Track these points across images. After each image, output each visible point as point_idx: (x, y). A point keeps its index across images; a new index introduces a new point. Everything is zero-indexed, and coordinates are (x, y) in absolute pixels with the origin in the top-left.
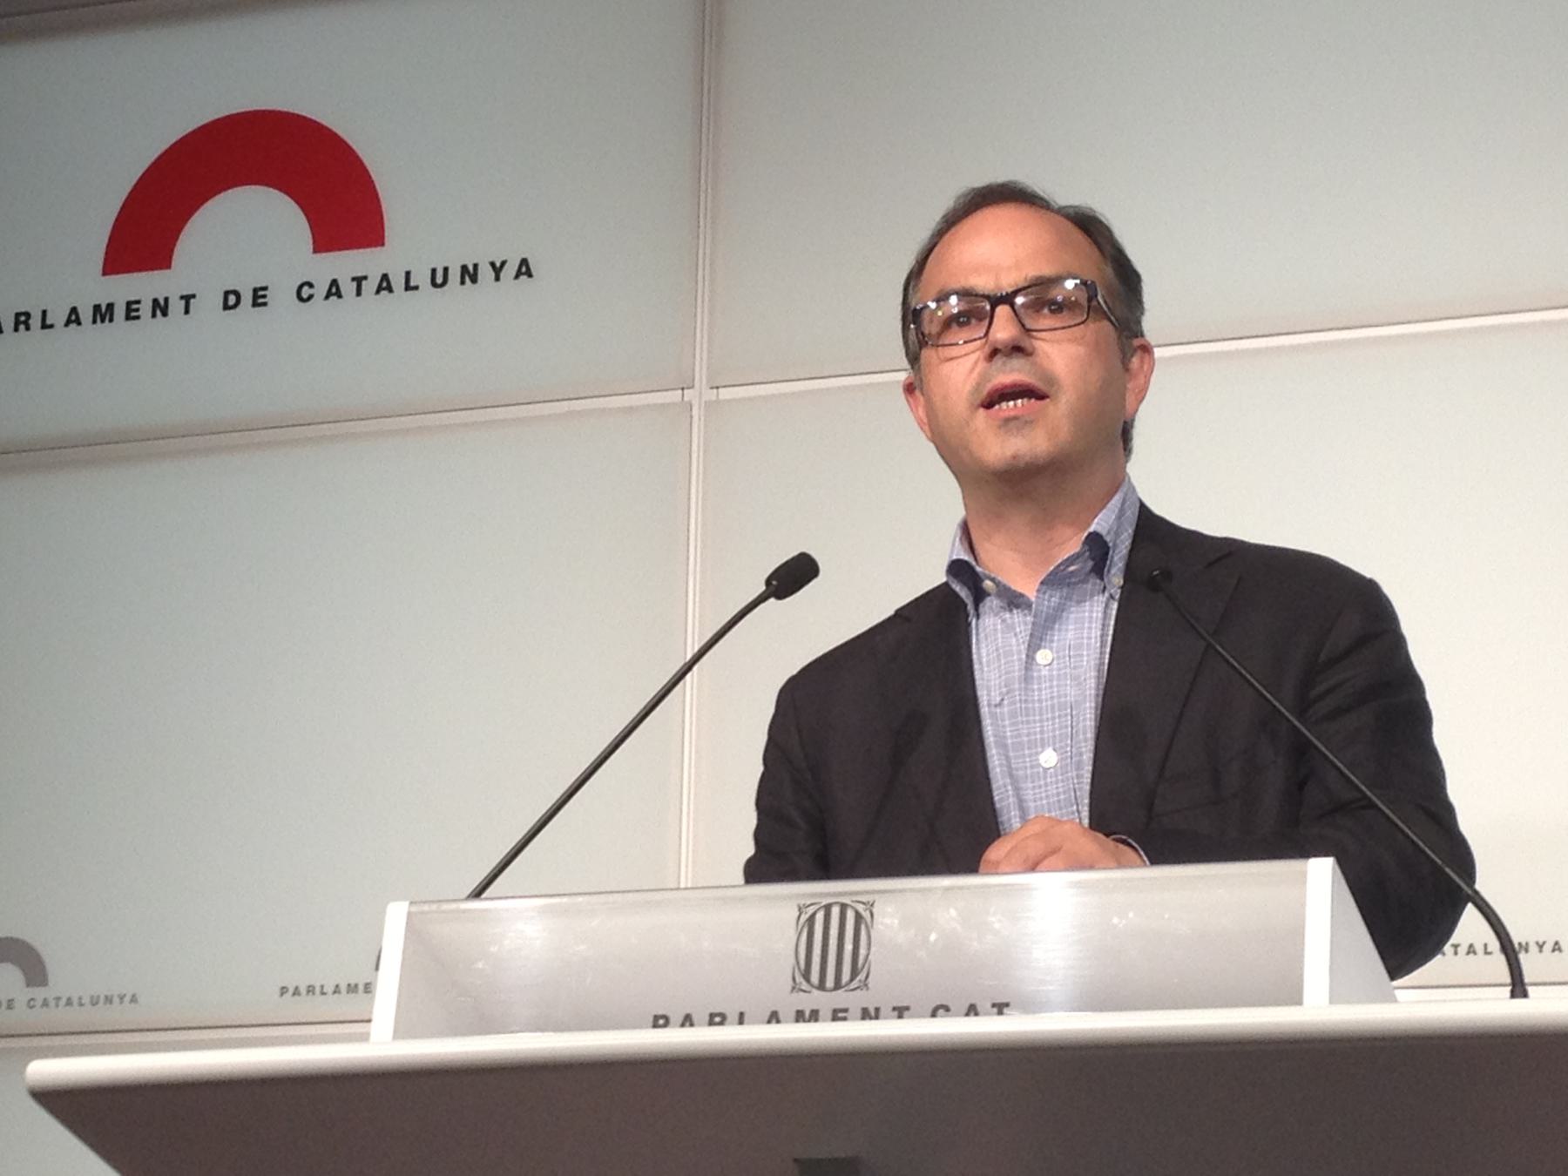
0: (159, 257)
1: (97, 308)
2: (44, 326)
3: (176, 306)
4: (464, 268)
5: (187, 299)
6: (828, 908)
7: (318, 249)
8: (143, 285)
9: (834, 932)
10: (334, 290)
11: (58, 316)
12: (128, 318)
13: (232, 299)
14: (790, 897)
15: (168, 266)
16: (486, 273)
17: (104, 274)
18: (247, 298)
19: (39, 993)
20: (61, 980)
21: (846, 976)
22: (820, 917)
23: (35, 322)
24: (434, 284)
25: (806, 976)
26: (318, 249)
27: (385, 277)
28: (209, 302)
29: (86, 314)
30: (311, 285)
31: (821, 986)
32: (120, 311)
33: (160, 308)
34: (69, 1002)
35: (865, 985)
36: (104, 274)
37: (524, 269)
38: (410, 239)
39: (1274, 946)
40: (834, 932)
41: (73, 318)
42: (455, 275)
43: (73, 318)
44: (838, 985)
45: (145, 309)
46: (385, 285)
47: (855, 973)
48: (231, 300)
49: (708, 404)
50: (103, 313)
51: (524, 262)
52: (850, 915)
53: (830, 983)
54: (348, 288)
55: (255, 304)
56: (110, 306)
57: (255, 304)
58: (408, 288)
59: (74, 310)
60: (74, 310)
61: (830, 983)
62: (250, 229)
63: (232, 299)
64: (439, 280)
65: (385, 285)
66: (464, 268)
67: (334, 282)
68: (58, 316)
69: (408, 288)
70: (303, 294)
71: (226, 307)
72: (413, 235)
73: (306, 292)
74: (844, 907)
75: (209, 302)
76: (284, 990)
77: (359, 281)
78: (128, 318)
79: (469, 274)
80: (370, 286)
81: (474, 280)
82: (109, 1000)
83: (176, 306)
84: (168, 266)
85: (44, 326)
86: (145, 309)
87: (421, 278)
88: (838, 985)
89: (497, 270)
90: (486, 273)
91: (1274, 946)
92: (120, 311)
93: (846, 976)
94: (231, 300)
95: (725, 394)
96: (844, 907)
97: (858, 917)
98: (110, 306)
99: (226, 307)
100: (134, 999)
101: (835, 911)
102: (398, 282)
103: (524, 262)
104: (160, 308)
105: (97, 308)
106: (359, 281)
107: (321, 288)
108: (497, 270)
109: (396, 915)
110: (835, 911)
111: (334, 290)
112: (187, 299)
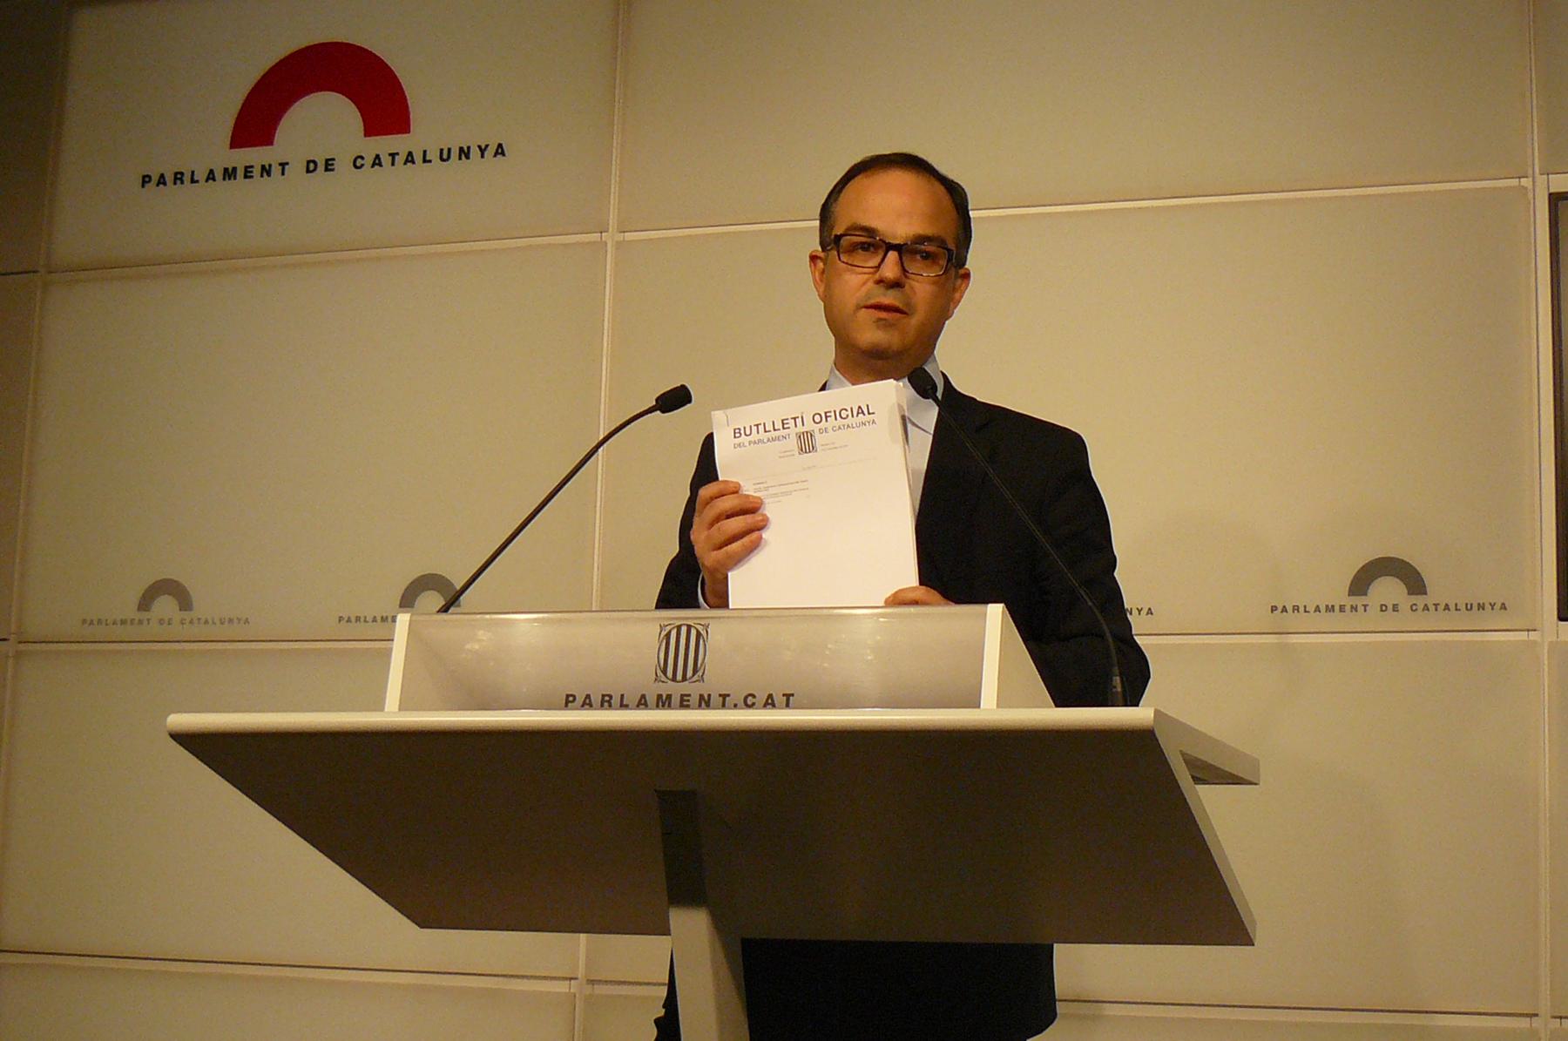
0: (267, 139)
1: (226, 170)
2: (193, 181)
3: (276, 170)
4: (461, 149)
5: (283, 165)
6: (679, 628)
7: (369, 132)
8: (254, 156)
10: (377, 162)
11: (201, 175)
13: (312, 166)
14: (654, 619)
15: (271, 143)
16: (475, 152)
19: (186, 615)
20: (201, 608)
21: (690, 673)
22: (674, 633)
23: (187, 178)
25: (664, 672)
26: (369, 132)
27: (410, 154)
29: (219, 174)
31: (674, 679)
32: (240, 173)
33: (266, 171)
34: (206, 622)
35: (702, 679)
37: (500, 151)
38: (425, 132)
41: (211, 176)
42: (455, 153)
43: (211, 176)
44: (684, 679)
45: (257, 171)
46: (410, 159)
47: (695, 671)
48: (311, 167)
50: (230, 174)
51: (500, 146)
52: (693, 632)
53: (679, 677)
54: (386, 160)
55: (327, 170)
56: (234, 169)
57: (327, 170)
58: (425, 161)
59: (211, 171)
60: (211, 171)
61: (679, 677)
62: (322, 120)
63: (312, 166)
64: (444, 157)
66: (461, 149)
67: (378, 157)
68: (201, 175)
69: (425, 161)
71: (308, 171)
73: (359, 162)
74: (689, 627)
76: (341, 619)
77: (393, 155)
79: (464, 153)
80: (400, 159)
81: (468, 157)
82: (231, 621)
83: (276, 170)
84: (271, 143)
85: (193, 181)
86: (257, 171)
89: (482, 151)
90: (475, 152)
92: (240, 173)
93: (690, 673)
94: (311, 167)
95: (629, 236)
96: (689, 627)
97: (699, 635)
98: (234, 169)
99: (308, 171)
100: (247, 621)
101: (684, 629)
102: (418, 157)
103: (500, 146)
104: (266, 171)
105: (226, 170)
107: (369, 160)
108: (482, 151)
110: (684, 629)
111: (377, 162)
112: (283, 165)
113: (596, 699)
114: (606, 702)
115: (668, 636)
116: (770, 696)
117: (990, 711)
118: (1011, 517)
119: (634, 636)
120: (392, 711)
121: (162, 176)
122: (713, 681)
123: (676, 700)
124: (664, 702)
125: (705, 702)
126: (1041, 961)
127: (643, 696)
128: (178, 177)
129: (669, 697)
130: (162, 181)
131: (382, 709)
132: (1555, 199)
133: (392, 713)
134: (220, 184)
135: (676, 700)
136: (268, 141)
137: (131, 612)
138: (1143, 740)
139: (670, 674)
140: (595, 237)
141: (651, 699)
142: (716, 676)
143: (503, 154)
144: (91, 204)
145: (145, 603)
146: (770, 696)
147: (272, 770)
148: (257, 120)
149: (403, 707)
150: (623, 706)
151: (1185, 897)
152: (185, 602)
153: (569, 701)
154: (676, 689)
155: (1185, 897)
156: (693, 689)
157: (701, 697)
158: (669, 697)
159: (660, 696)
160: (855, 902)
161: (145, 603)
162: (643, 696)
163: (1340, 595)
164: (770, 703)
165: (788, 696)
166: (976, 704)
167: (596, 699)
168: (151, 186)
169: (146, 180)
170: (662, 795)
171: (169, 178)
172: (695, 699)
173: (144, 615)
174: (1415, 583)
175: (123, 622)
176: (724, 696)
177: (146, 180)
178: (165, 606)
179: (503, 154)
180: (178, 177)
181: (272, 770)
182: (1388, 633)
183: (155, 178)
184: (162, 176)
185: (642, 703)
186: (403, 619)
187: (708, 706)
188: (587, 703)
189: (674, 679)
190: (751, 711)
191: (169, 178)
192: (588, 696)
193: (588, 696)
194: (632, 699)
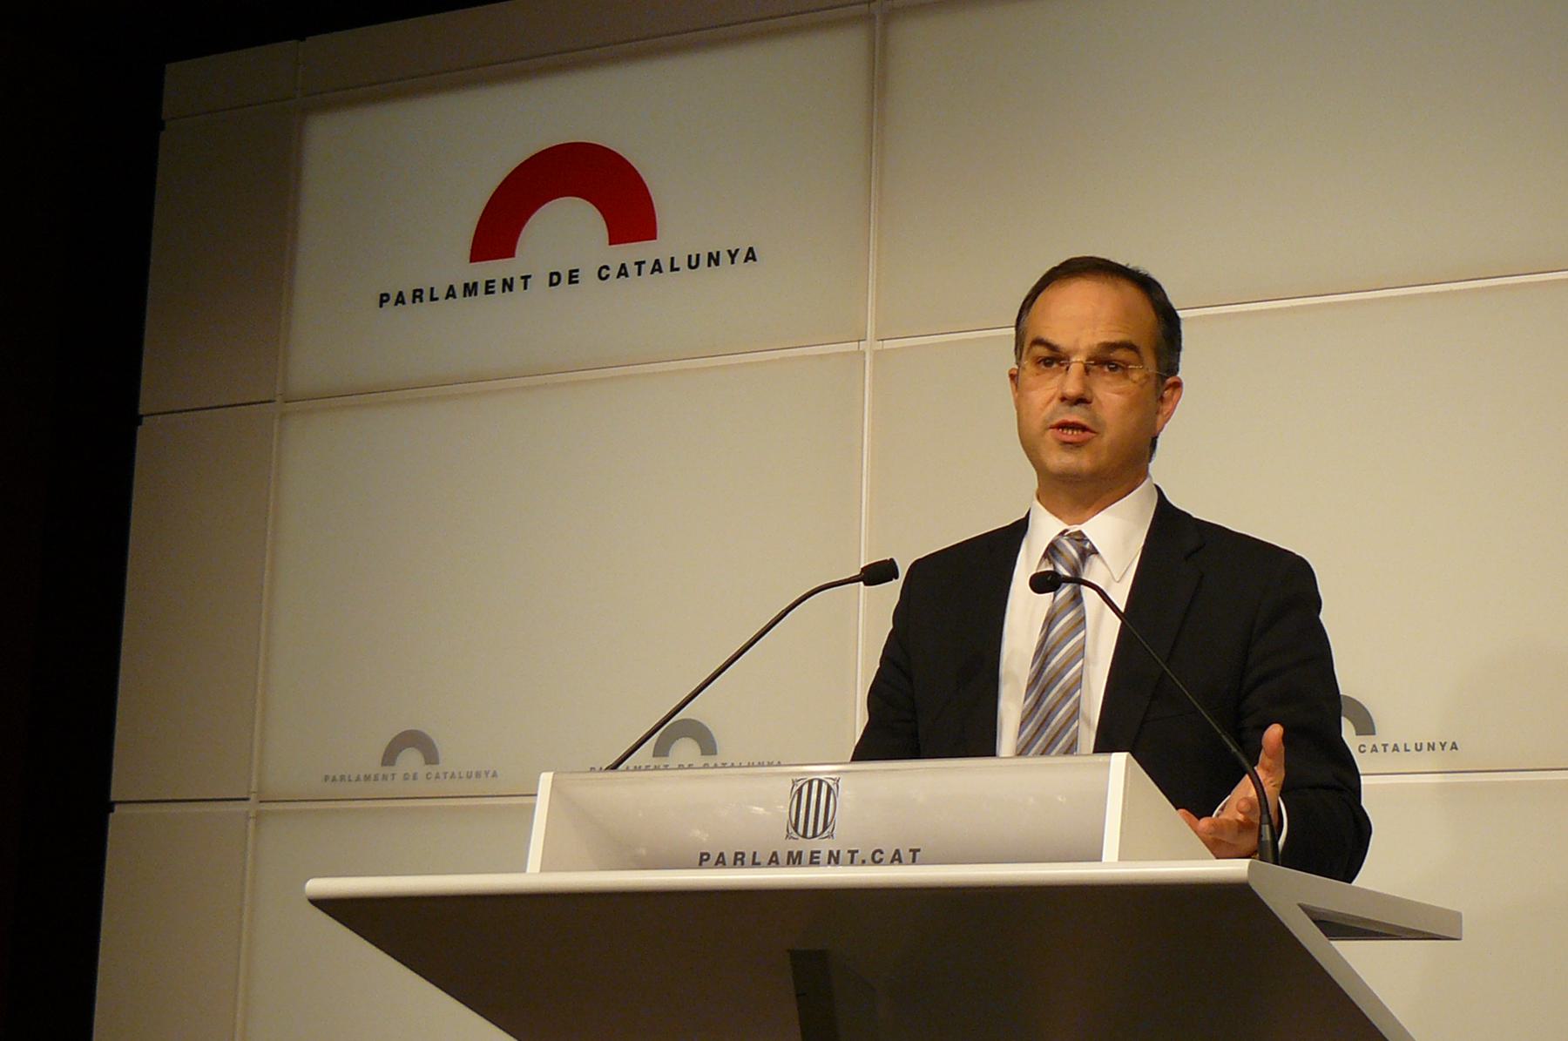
1: (466, 285)
2: (433, 299)
3: (518, 284)
4: (710, 255)
5: (526, 278)
6: (811, 782)
7: (614, 239)
8: (496, 269)
9: (814, 796)
11: (441, 292)
12: (487, 292)
13: (555, 278)
17: (472, 261)
18: (565, 278)
20: (447, 762)
22: (805, 788)
23: (426, 296)
24: (690, 267)
25: (796, 828)
26: (614, 239)
27: (657, 262)
29: (459, 290)
30: (607, 268)
31: (804, 836)
32: (481, 288)
33: (508, 285)
34: (453, 776)
36: (472, 261)
37: (751, 255)
40: (814, 796)
41: (451, 293)
42: (704, 259)
43: (451, 293)
44: (814, 836)
45: (498, 286)
46: (657, 267)
47: (825, 827)
48: (554, 279)
49: (877, 354)
50: (470, 289)
51: (751, 250)
52: (824, 787)
53: (810, 834)
56: (475, 284)
58: (673, 269)
59: (451, 287)
60: (451, 287)
61: (810, 834)
62: (567, 228)
63: (555, 278)
65: (657, 267)
67: (623, 266)
68: (441, 292)
69: (673, 269)
71: (551, 284)
72: (678, 230)
75: (540, 281)
77: (640, 264)
78: (487, 292)
79: (714, 259)
80: (647, 268)
81: (717, 263)
82: (478, 775)
83: (518, 284)
86: (498, 286)
87: (681, 262)
88: (814, 836)
89: (733, 256)
92: (481, 288)
95: (888, 344)
96: (820, 782)
97: (829, 789)
98: (475, 284)
99: (551, 284)
100: (495, 775)
101: (815, 784)
102: (666, 266)
103: (751, 250)
104: (508, 285)
105: (466, 285)
106: (640, 264)
110: (815, 784)
111: (623, 271)
113: (729, 857)
114: (739, 860)
115: (800, 791)
116: (897, 852)
117: (1113, 864)
120: (535, 872)
121: (400, 294)
122: (841, 838)
123: (806, 857)
124: (794, 859)
125: (834, 859)
127: (775, 854)
128: (417, 295)
129: (800, 854)
130: (400, 299)
131: (524, 871)
133: (534, 875)
135: (806, 857)
136: (509, 252)
137: (374, 766)
139: (801, 830)
140: (853, 346)
141: (783, 857)
143: (754, 259)
144: (329, 325)
145: (389, 757)
146: (897, 852)
147: (421, 933)
148: (496, 234)
149: (545, 868)
150: (755, 864)
152: (431, 756)
153: (703, 860)
154: (806, 846)
156: (824, 846)
157: (831, 853)
158: (800, 854)
159: (790, 853)
161: (389, 757)
162: (775, 854)
164: (897, 858)
165: (914, 851)
166: (1097, 857)
167: (729, 857)
168: (389, 305)
169: (384, 298)
170: (795, 955)
171: (408, 297)
172: (824, 856)
173: (388, 770)
175: (367, 778)
176: (853, 853)
177: (384, 298)
178: (411, 759)
179: (754, 259)
180: (417, 295)
183: (393, 298)
184: (400, 294)
185: (774, 861)
187: (837, 863)
188: (721, 862)
189: (804, 836)
190: (757, 870)
191: (408, 297)
192: (721, 854)
193: (721, 854)
194: (763, 857)
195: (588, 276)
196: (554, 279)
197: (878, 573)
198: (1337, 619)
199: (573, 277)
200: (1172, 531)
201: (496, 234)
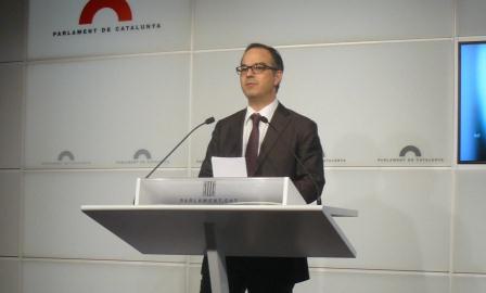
8: (86, 27)
20: (76, 160)
28: (99, 31)
33: (90, 31)
37: (159, 26)
38: (138, 16)
39: (282, 194)
41: (74, 33)
43: (74, 33)
50: (79, 32)
64: (143, 27)
70: (117, 29)
75: (99, 31)
79: (148, 26)
91: (282, 194)
94: (103, 30)
104: (90, 31)
109: (139, 180)
117: (285, 206)
118: (295, 150)
119: (197, 185)
126: (304, 262)
128: (64, 33)
132: (460, 44)
133: (137, 206)
134: (77, 35)
138: (319, 214)
142: (220, 191)
144: (39, 39)
145: (60, 158)
147: (106, 218)
148: (87, 16)
149: (140, 203)
151: (337, 247)
152: (72, 158)
153: (182, 201)
155: (337, 247)
160: (254, 247)
161: (60, 158)
163: (397, 156)
166: (281, 202)
169: (54, 34)
174: (418, 153)
177: (54, 34)
178: (66, 159)
180: (64, 33)
181: (106, 218)
182: (410, 166)
186: (139, 180)
195: (113, 30)
196: (103, 30)
197: (210, 121)
198: (321, 133)
199: (109, 30)
200: (281, 108)
201: (87, 16)
